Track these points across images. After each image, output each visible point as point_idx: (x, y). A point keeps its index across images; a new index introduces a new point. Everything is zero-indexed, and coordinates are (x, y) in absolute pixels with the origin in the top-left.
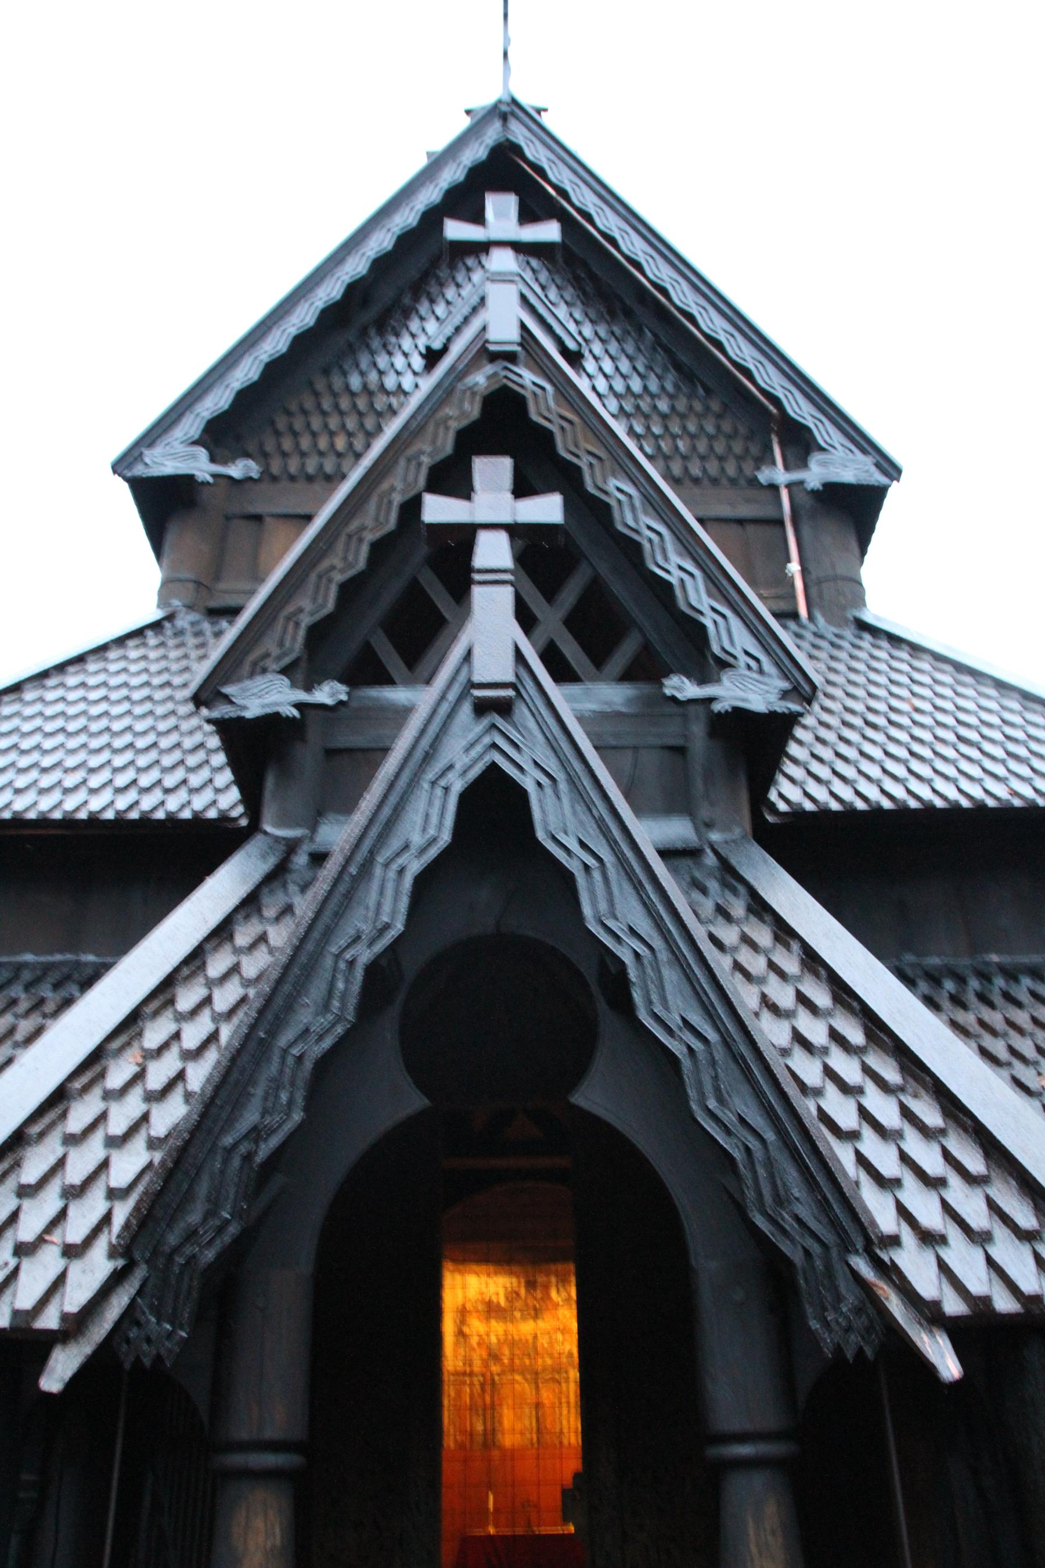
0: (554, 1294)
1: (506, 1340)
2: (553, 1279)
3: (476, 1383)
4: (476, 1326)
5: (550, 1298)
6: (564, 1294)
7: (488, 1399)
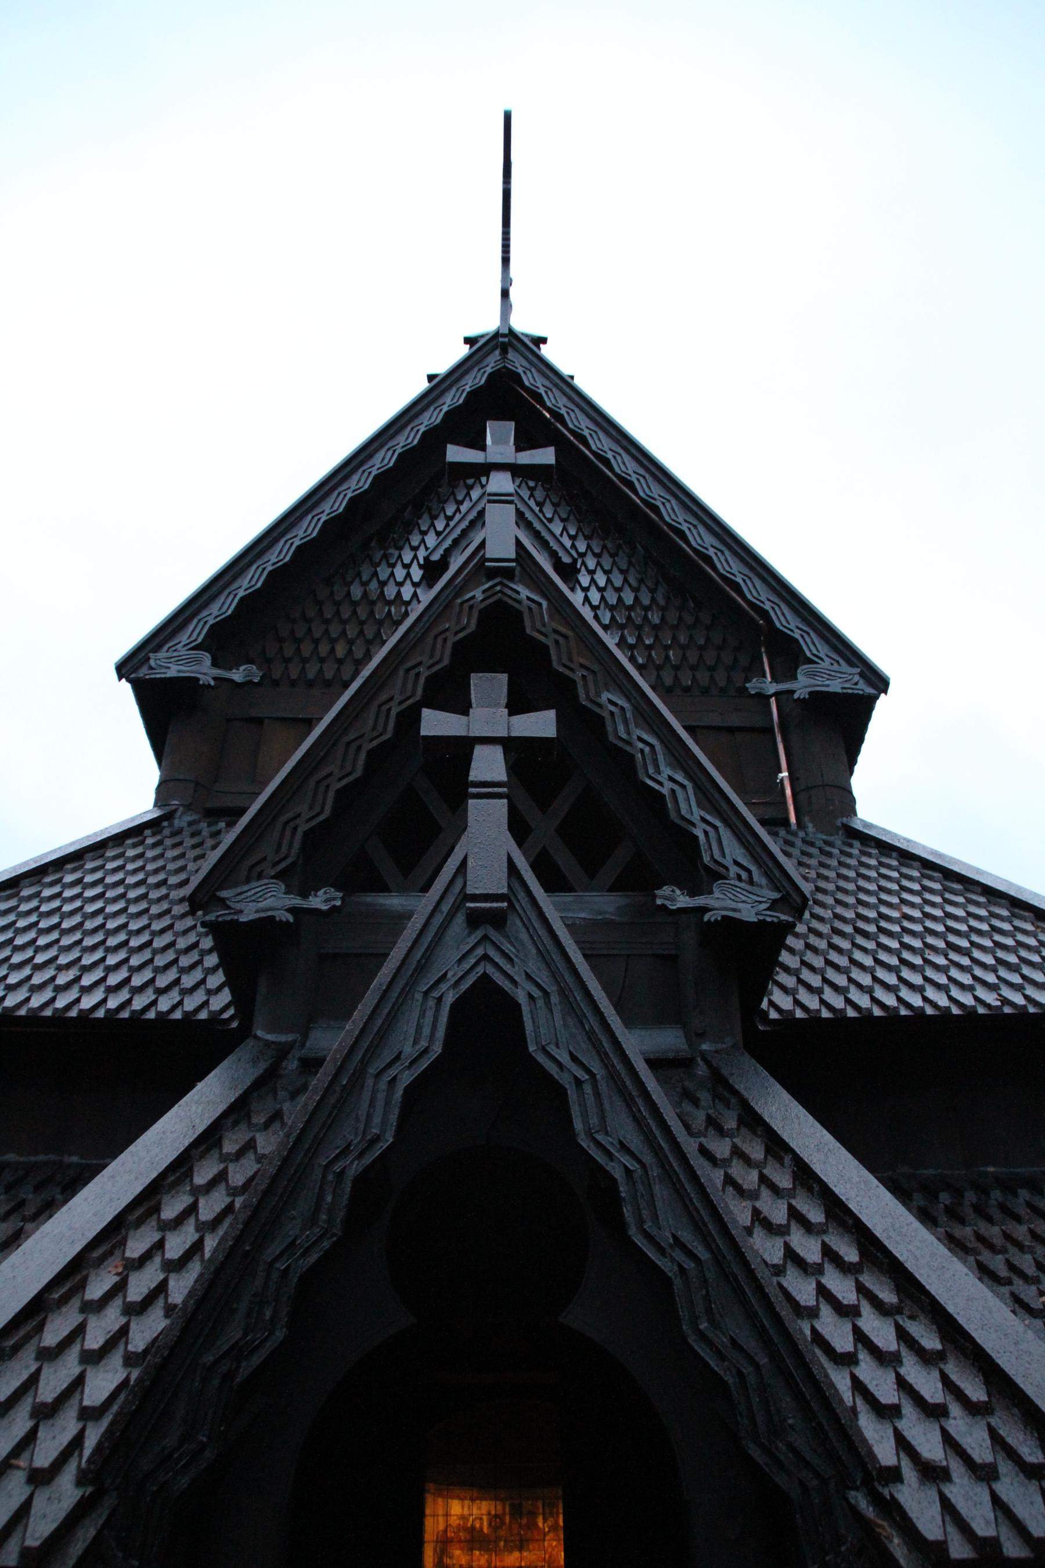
2: (540, 1504)
5: (536, 1525)
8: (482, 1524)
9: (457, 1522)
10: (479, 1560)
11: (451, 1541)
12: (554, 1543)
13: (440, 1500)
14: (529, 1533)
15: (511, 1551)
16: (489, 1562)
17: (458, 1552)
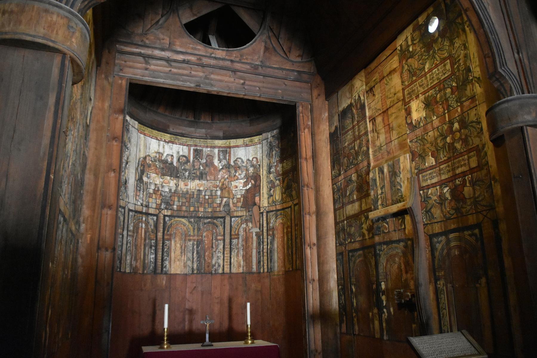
0: (216, 162)
1: (176, 190)
3: (151, 222)
5: (212, 164)
6: (224, 162)
7: (160, 235)
8: (172, 159)
9: (155, 155)
10: (169, 183)
11: (149, 166)
12: (226, 177)
13: (142, 136)
14: (207, 169)
15: (193, 179)
16: (177, 185)
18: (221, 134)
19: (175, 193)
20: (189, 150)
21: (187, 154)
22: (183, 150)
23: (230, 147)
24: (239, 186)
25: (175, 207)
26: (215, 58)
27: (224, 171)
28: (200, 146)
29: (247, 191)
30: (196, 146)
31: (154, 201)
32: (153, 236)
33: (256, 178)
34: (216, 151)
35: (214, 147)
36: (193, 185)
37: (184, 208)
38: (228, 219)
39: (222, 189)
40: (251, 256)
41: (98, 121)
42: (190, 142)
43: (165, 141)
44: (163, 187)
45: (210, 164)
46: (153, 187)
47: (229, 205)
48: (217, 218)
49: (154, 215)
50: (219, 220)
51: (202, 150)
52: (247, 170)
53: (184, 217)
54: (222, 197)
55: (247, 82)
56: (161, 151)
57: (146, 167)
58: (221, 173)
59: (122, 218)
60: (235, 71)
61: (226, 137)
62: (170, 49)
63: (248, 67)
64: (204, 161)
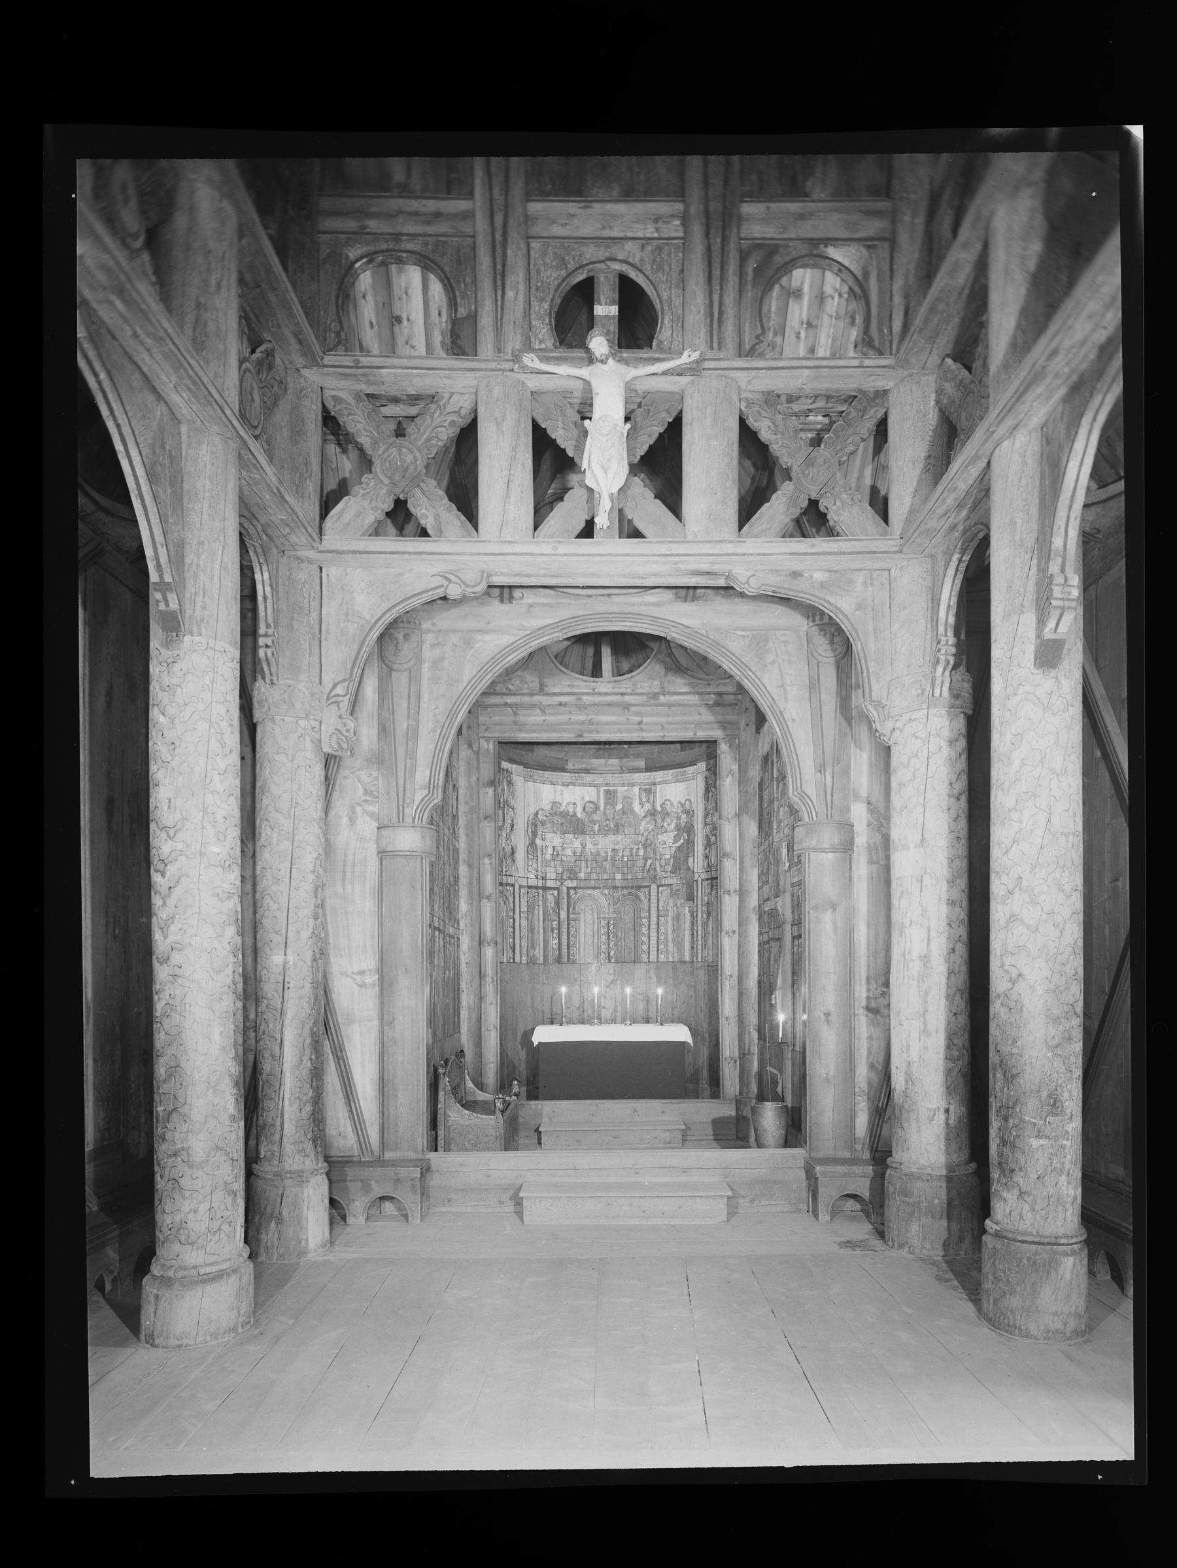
0: (636, 807)
1: (582, 852)
3: (551, 899)
4: (551, 840)
5: (632, 811)
6: (648, 806)
7: (563, 914)
10: (572, 842)
11: (543, 823)
16: (584, 846)
17: (549, 836)
18: (641, 763)
19: (580, 856)
20: (598, 792)
21: (595, 800)
22: (589, 793)
23: (655, 784)
24: (667, 843)
25: (582, 875)
26: (600, 694)
27: (648, 819)
28: (614, 785)
29: (679, 847)
30: (607, 785)
31: (553, 870)
32: (554, 916)
33: (689, 829)
34: (636, 789)
35: (633, 785)
36: (606, 843)
37: (594, 876)
38: (654, 887)
39: (645, 847)
40: (683, 939)
41: (466, 803)
42: (599, 780)
43: (564, 784)
44: (563, 849)
45: (627, 810)
46: (550, 851)
47: (655, 870)
48: (639, 888)
49: (554, 889)
50: (643, 890)
51: (615, 791)
52: (678, 818)
53: (595, 888)
54: (645, 859)
55: (645, 719)
56: (558, 799)
57: (539, 824)
58: (643, 823)
59: (511, 899)
60: (627, 707)
61: (648, 769)
62: (542, 690)
63: (645, 698)
64: (619, 807)
